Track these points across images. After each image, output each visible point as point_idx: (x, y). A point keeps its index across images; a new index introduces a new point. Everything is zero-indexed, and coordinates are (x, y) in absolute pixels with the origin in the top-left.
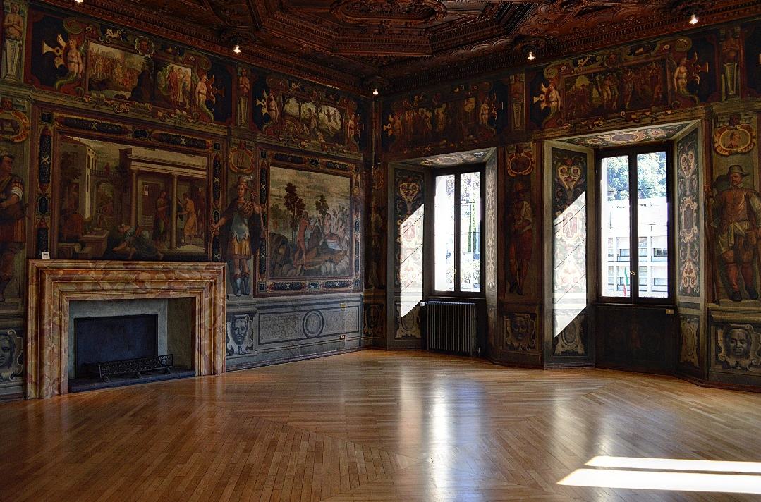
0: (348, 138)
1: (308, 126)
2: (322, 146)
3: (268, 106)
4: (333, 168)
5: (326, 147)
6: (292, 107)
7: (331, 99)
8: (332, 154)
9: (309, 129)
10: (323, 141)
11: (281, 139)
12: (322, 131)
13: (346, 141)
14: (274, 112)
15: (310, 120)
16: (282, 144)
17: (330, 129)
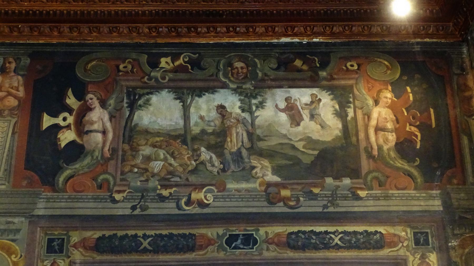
0: (370, 156)
1: (218, 148)
2: (270, 194)
3: (80, 126)
4: (316, 248)
5: (285, 193)
6: (161, 112)
7: (299, 70)
8: (315, 207)
9: (220, 155)
10: (271, 178)
11: (118, 197)
12: (269, 154)
13: (365, 165)
14: (99, 137)
15: (223, 133)
16: (123, 209)
17: (300, 145)
